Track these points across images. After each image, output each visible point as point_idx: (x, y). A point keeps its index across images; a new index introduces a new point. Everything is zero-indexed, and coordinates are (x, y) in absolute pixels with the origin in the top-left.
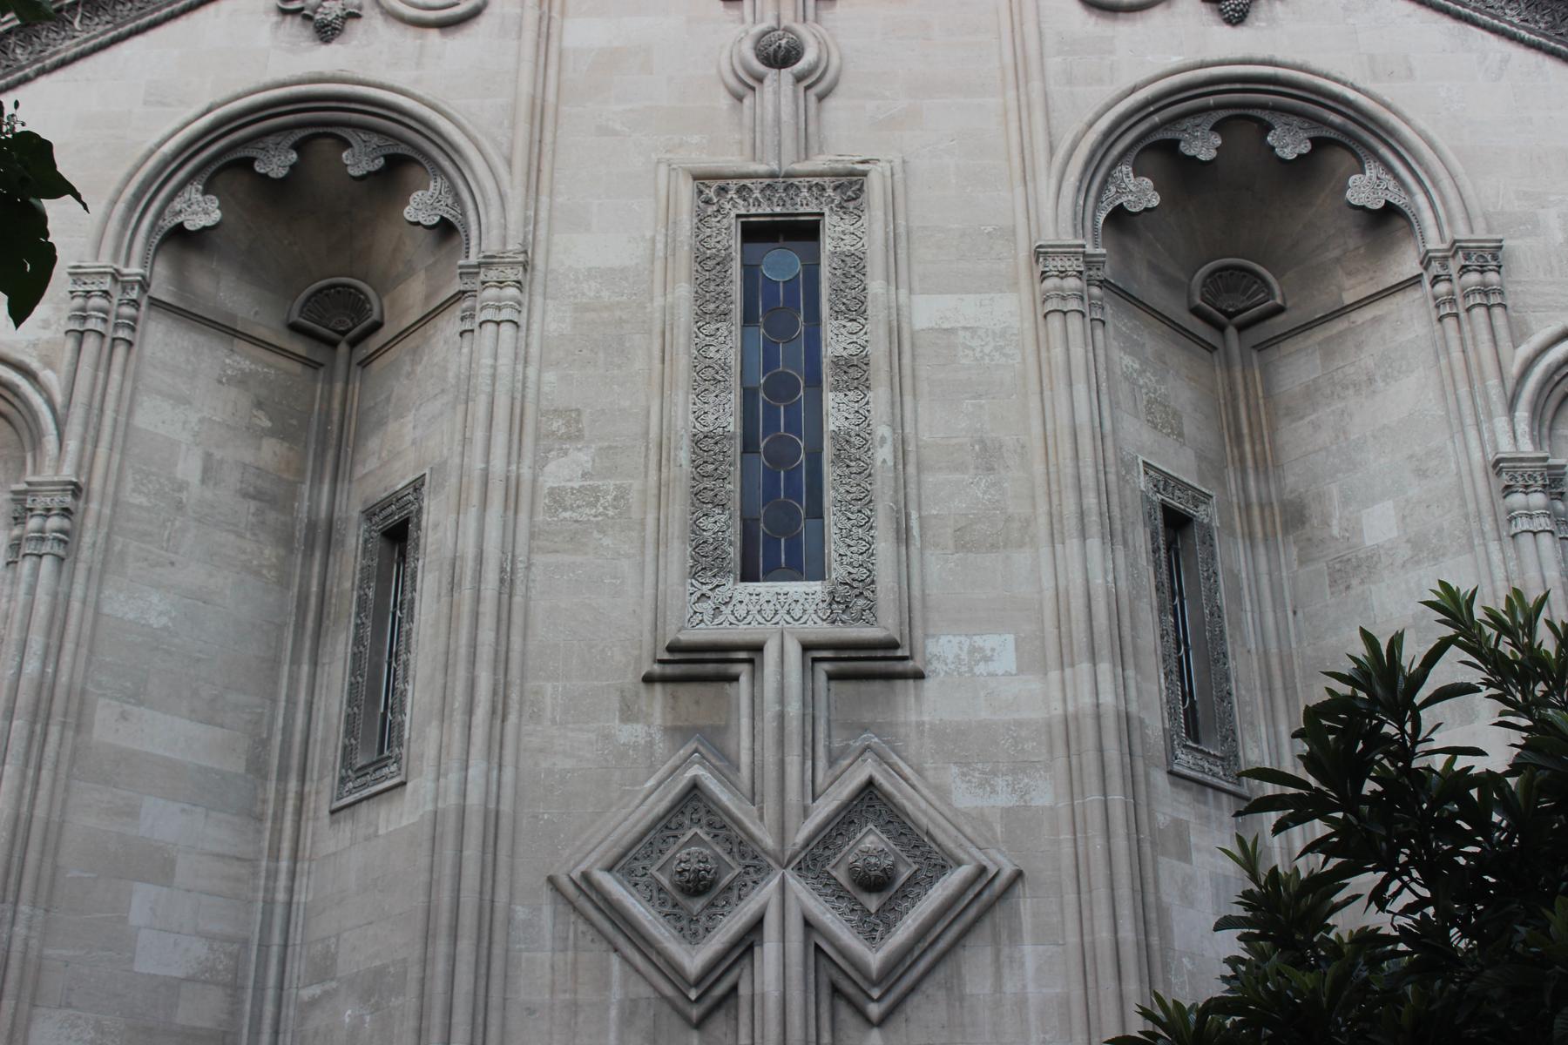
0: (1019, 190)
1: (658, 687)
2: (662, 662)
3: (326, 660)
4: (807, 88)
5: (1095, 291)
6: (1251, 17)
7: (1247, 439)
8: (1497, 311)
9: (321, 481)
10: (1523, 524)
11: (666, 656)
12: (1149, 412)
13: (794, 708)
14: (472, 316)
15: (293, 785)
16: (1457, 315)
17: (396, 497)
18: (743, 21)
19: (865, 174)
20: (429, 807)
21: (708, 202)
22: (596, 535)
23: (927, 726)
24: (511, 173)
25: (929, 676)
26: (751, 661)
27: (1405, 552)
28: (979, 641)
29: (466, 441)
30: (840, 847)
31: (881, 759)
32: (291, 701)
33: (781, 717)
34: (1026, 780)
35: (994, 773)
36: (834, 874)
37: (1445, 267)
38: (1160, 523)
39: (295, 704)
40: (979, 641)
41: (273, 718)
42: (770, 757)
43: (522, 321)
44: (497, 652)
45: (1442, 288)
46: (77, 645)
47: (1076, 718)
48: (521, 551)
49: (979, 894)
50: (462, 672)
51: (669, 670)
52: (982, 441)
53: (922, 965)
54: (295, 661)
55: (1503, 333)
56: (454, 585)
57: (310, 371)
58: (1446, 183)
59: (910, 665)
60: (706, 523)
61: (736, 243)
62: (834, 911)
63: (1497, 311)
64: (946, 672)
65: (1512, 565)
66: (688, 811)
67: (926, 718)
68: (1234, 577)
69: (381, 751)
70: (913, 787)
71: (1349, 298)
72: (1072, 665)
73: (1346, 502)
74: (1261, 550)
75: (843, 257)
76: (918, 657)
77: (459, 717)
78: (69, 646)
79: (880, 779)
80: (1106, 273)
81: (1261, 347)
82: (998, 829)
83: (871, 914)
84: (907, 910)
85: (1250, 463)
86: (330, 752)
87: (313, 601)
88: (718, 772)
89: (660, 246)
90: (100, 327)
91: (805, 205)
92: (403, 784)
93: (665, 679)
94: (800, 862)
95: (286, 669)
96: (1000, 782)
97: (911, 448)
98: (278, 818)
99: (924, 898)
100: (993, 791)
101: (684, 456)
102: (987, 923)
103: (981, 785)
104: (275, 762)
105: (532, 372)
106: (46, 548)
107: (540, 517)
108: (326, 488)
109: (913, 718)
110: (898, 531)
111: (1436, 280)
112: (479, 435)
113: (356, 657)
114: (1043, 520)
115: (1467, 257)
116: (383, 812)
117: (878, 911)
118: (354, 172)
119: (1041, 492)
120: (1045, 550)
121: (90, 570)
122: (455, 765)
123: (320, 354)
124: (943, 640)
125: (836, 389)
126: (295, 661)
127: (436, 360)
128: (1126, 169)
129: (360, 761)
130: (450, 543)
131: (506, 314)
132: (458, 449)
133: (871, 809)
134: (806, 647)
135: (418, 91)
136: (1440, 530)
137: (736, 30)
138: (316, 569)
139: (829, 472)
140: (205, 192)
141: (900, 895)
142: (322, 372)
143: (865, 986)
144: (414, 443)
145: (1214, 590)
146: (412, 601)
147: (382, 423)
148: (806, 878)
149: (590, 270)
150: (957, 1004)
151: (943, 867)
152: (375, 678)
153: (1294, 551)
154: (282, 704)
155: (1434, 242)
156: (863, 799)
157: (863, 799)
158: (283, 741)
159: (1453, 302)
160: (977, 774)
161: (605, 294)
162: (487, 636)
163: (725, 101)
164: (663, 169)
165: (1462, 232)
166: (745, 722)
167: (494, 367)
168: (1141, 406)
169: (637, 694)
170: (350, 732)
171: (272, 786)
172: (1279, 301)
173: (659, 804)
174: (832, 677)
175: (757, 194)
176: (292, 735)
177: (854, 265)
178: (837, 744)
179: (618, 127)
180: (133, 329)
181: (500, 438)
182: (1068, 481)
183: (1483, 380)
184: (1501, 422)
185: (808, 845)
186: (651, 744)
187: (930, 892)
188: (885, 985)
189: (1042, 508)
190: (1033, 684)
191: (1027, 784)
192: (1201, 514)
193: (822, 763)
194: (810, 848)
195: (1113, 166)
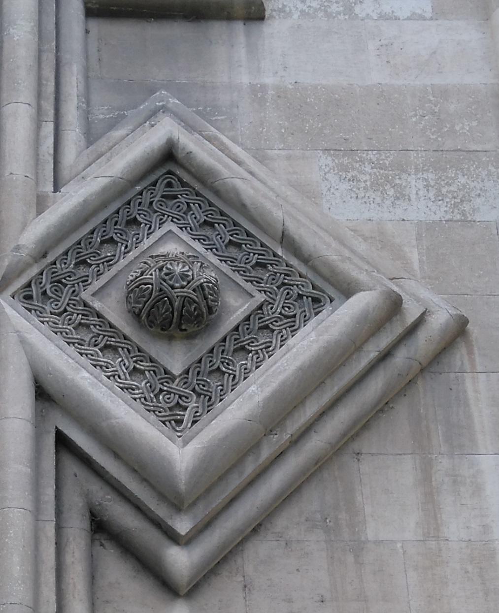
23: (271, 92)
25: (271, 17)
30: (109, 262)
34: (462, 180)
35: (401, 168)
36: (97, 305)
49: (386, 355)
53: (277, 480)
62: (98, 371)
64: (302, 11)
67: (269, 80)
79: (188, 142)
82: (414, 256)
83: (173, 378)
84: (247, 373)
94: (29, 285)
96: (413, 183)
99: (278, 352)
100: (401, 195)
102: (401, 411)
103: (376, 185)
109: (245, 79)
117: (187, 372)
133: (171, 203)
141: (230, 346)
143: (161, 511)
148: (39, 313)
150: (350, 559)
151: (316, 300)
156: (154, 184)
157: (154, 184)
160: (368, 169)
185: (44, 256)
187: (291, 341)
188: (202, 511)
191: (464, 186)
194: (50, 259)
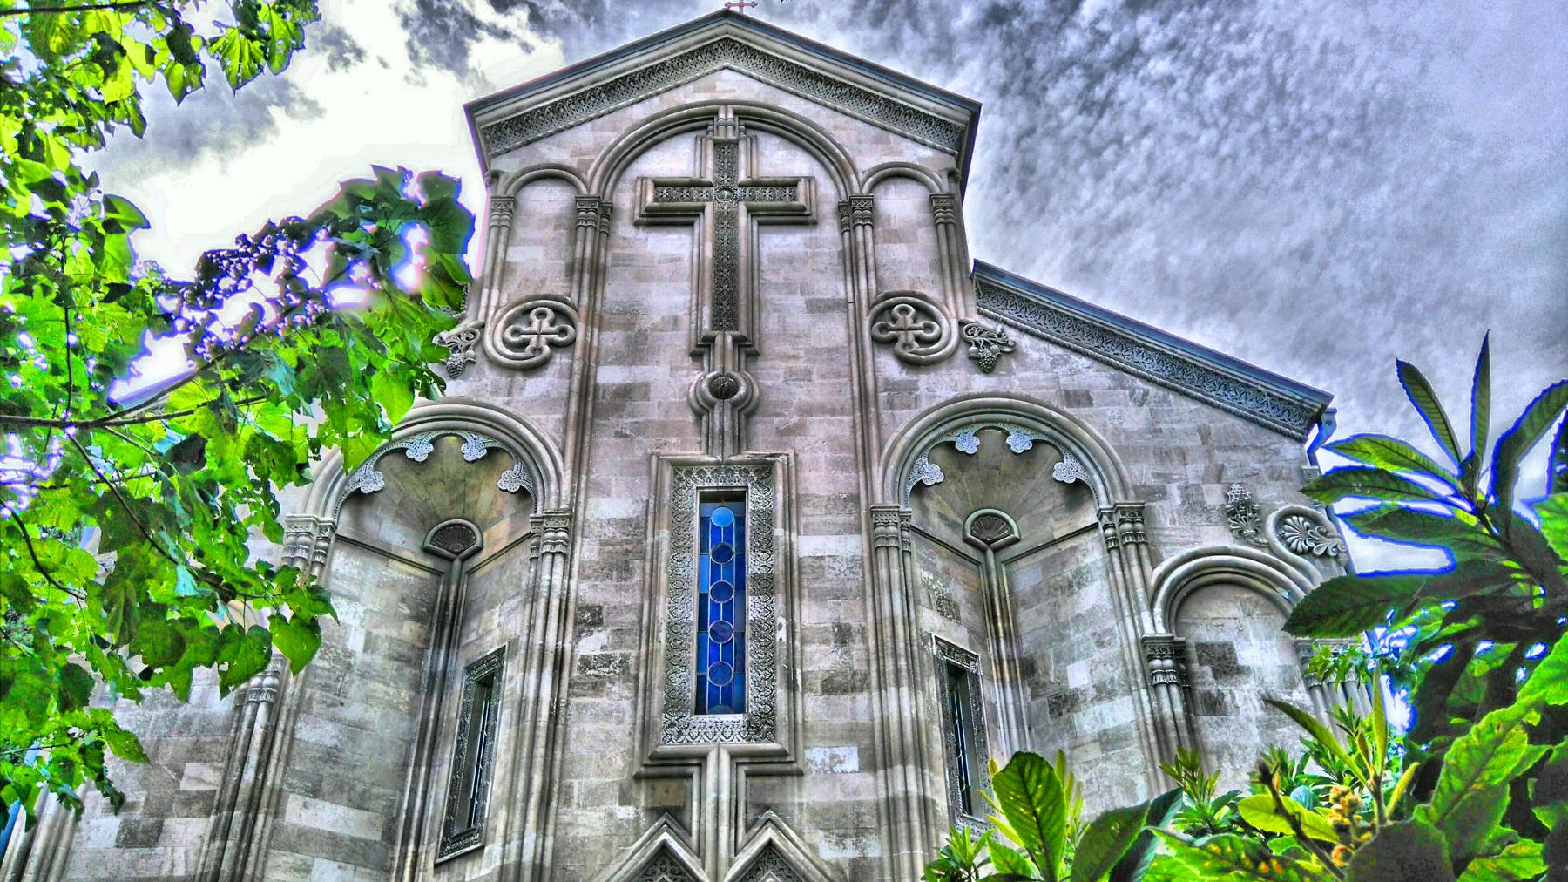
0: (862, 474)
1: (643, 783)
2: (646, 766)
3: (437, 763)
4: (740, 411)
5: (906, 534)
6: (997, 367)
7: (999, 620)
8: (1142, 547)
9: (440, 647)
10: (1160, 679)
11: (649, 762)
12: (939, 605)
13: (725, 796)
14: (538, 549)
15: (411, 848)
16: (1118, 548)
17: (486, 659)
18: (703, 369)
19: (772, 463)
20: (498, 863)
21: (681, 479)
22: (609, 685)
24: (564, 461)
26: (699, 765)
27: (1092, 692)
28: (836, 751)
29: (531, 627)
31: (777, 827)
32: (413, 791)
33: (717, 801)
35: (845, 836)
37: (1110, 519)
38: (945, 675)
39: (416, 793)
40: (836, 751)
41: (401, 803)
42: (710, 827)
43: (568, 552)
44: (545, 761)
45: (1109, 531)
46: (279, 760)
47: (894, 800)
48: (564, 695)
50: (522, 776)
51: (651, 771)
52: (839, 626)
54: (418, 765)
55: (1146, 561)
56: (521, 718)
57: (435, 577)
58: (1111, 469)
59: (795, 766)
60: (674, 678)
61: (696, 505)
63: (1142, 547)
65: (1154, 704)
66: (659, 863)
67: (804, 800)
68: (993, 706)
69: (469, 825)
70: (796, 845)
71: (1057, 535)
72: (891, 766)
73: (1058, 660)
74: (1009, 689)
75: (758, 513)
76: (800, 761)
77: (519, 805)
78: (274, 761)
79: (776, 840)
80: (913, 522)
81: (1008, 562)
85: (1001, 635)
86: (436, 825)
87: (431, 725)
88: (677, 837)
89: (651, 506)
90: (305, 555)
91: (737, 482)
92: (482, 848)
93: (648, 778)
95: (411, 769)
97: (798, 630)
98: (401, 869)
101: (662, 636)
104: (401, 832)
105: (573, 583)
106: (262, 698)
107: (575, 674)
108: (443, 652)
110: (788, 682)
111: (1105, 527)
112: (540, 623)
113: (457, 762)
114: (874, 675)
115: (1123, 514)
116: (469, 865)
118: (470, 459)
119: (873, 657)
120: (875, 694)
121: (289, 711)
122: (516, 836)
123: (442, 567)
124: (815, 750)
125: (753, 594)
126: (418, 765)
127: (515, 573)
128: (924, 459)
129: (456, 831)
130: (519, 692)
131: (558, 548)
132: (526, 631)
134: (734, 756)
135: (509, 409)
136: (1112, 680)
137: (698, 375)
138: (434, 704)
139: (749, 645)
140: (375, 469)
142: (443, 578)
144: (499, 625)
145: (980, 714)
146: (494, 726)
147: (480, 612)
149: (609, 520)
152: (468, 775)
153: (1028, 690)
154: (407, 793)
155: (1104, 505)
158: (407, 818)
159: (1116, 540)
161: (618, 535)
162: (540, 751)
163: (690, 418)
164: (654, 459)
165: (1120, 499)
166: (695, 804)
167: (550, 581)
168: (934, 602)
169: (630, 787)
170: (450, 812)
171: (398, 848)
172: (1017, 535)
173: (641, 859)
174: (748, 775)
175: (709, 475)
176: (412, 812)
177: (766, 519)
178: (751, 817)
179: (628, 432)
180: (325, 556)
181: (553, 625)
182: (889, 651)
183: (1134, 589)
184: (1145, 615)
186: (637, 819)
189: (874, 668)
190: (868, 778)
192: (971, 667)
193: (741, 830)
195: (917, 458)
